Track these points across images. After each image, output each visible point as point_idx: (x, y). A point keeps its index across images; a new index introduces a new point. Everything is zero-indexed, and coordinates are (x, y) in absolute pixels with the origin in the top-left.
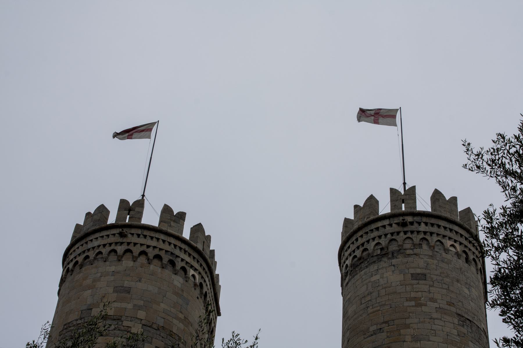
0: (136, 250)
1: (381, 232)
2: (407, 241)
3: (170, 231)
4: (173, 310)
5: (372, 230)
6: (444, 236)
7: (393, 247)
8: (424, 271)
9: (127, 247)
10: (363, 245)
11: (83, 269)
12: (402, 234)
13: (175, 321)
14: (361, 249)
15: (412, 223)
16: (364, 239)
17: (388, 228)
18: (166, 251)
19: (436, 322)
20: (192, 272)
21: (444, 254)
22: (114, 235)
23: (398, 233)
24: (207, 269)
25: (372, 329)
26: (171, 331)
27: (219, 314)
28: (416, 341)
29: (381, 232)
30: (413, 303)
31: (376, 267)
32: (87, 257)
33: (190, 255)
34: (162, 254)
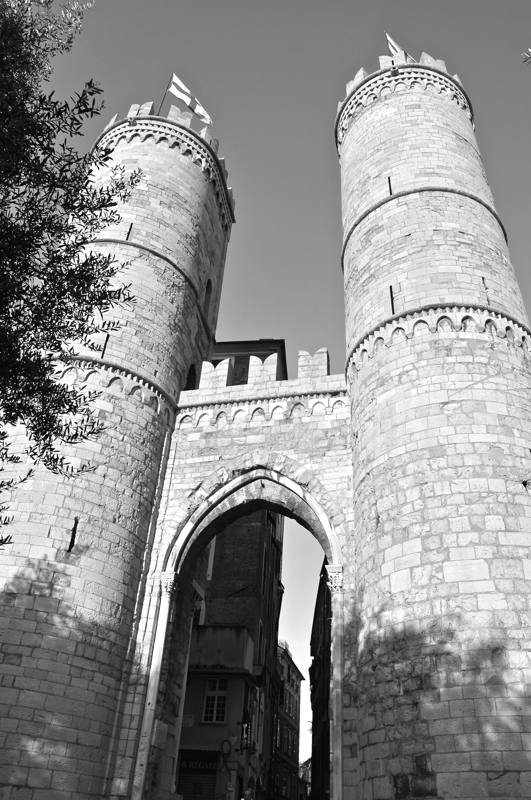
0: (143, 134)
3: (175, 121)
4: (178, 178)
6: (435, 82)
7: (387, 92)
8: (418, 103)
13: (181, 187)
14: (355, 106)
15: (403, 74)
18: (172, 136)
23: (390, 82)
25: (369, 153)
27: (234, 221)
30: (410, 124)
31: (370, 111)
34: (168, 137)
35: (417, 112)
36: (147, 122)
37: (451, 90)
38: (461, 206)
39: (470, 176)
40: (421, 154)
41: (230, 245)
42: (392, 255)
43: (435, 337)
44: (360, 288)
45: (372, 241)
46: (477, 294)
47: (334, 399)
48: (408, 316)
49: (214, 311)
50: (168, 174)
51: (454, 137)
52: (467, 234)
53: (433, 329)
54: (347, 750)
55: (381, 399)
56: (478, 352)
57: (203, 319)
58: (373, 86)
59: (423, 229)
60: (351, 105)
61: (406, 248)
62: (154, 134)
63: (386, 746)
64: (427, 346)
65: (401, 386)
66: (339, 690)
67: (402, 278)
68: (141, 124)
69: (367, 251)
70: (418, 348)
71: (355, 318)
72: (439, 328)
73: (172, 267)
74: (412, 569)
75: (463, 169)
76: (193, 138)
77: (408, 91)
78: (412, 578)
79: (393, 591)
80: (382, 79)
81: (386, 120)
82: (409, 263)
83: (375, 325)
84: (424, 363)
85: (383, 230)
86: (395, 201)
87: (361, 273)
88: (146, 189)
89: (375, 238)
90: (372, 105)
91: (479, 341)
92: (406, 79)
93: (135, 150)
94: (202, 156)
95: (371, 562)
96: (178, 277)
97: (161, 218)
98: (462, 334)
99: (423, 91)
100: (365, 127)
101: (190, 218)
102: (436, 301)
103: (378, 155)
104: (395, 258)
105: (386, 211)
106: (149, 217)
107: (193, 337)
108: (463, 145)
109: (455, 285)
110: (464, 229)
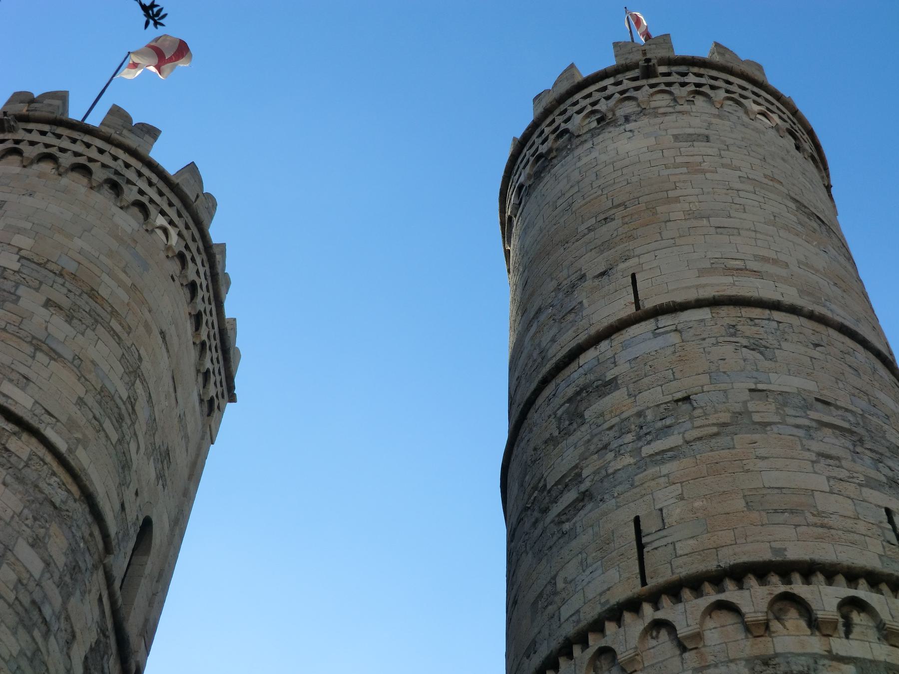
0: (30, 152)
2: (659, 96)
3: (116, 136)
7: (629, 108)
8: (703, 131)
13: (105, 277)
14: (552, 137)
15: (668, 74)
18: (104, 166)
19: (742, 194)
20: (161, 221)
21: (745, 118)
23: (637, 89)
25: (583, 228)
26: (93, 289)
27: (232, 398)
30: (685, 170)
31: (588, 145)
33: (161, 194)
35: (701, 147)
36: (46, 128)
37: (780, 117)
38: (817, 345)
39: (834, 288)
40: (713, 230)
41: (213, 450)
42: (640, 444)
43: (764, 646)
44: (555, 529)
45: (587, 414)
48: (686, 593)
49: (151, 604)
50: (78, 243)
51: (793, 205)
52: (838, 407)
53: (757, 624)
57: (115, 612)
58: (596, 96)
59: (723, 386)
60: (544, 136)
62: (59, 154)
67: (665, 497)
68: (30, 131)
69: (572, 439)
71: (535, 603)
72: (775, 625)
73: (49, 458)
75: (817, 271)
76: (155, 179)
77: (679, 108)
80: (617, 84)
81: (627, 162)
82: (686, 462)
83: (590, 614)
85: (617, 388)
86: (650, 325)
87: (554, 494)
88: (16, 266)
90: (593, 133)
92: (677, 86)
94: (171, 223)
96: (62, 485)
97: (42, 335)
98: (839, 645)
99: (716, 112)
100: (576, 176)
101: (119, 352)
102: (761, 553)
103: (605, 231)
104: (647, 450)
105: (625, 346)
106: (10, 328)
107: (79, 653)
108: (815, 225)
109: (812, 519)
110: (828, 395)
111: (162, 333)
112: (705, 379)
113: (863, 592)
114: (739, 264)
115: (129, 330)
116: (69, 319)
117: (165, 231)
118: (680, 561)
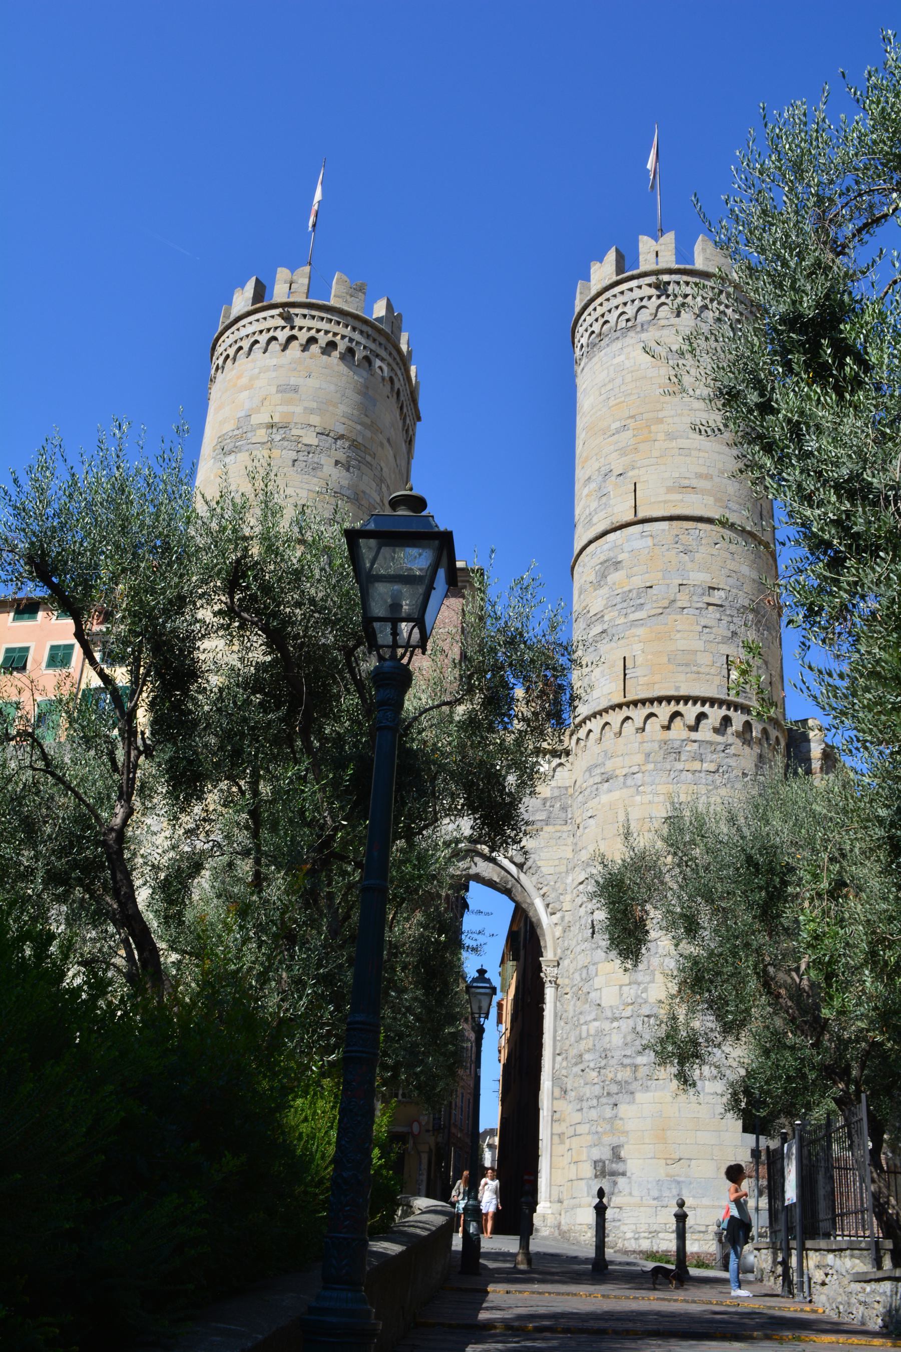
0: (303, 336)
1: (628, 297)
3: (346, 308)
5: (615, 296)
7: (644, 316)
9: (291, 333)
10: (603, 315)
11: (237, 363)
12: (654, 299)
14: (601, 321)
16: (605, 309)
17: (636, 291)
18: (343, 337)
20: (378, 363)
22: (273, 317)
23: (650, 298)
24: (398, 359)
27: (419, 419)
28: (671, 439)
29: (628, 297)
32: (241, 348)
41: (414, 462)
46: (717, 680)
47: (556, 761)
52: (718, 589)
54: (556, 1138)
55: (604, 798)
56: (710, 757)
59: (668, 581)
61: (646, 607)
63: (589, 1137)
64: (656, 746)
65: (625, 790)
66: (550, 1083)
67: (637, 649)
70: (647, 747)
74: (621, 986)
78: (621, 995)
79: (603, 1005)
84: (651, 766)
89: (614, 577)
91: (711, 743)
93: (293, 365)
95: (585, 971)
98: (694, 735)
104: (632, 617)
111: (388, 440)
112: (660, 574)
113: (707, 708)
114: (686, 483)
115: (374, 456)
116: (348, 470)
117: (380, 368)
118: (639, 688)
